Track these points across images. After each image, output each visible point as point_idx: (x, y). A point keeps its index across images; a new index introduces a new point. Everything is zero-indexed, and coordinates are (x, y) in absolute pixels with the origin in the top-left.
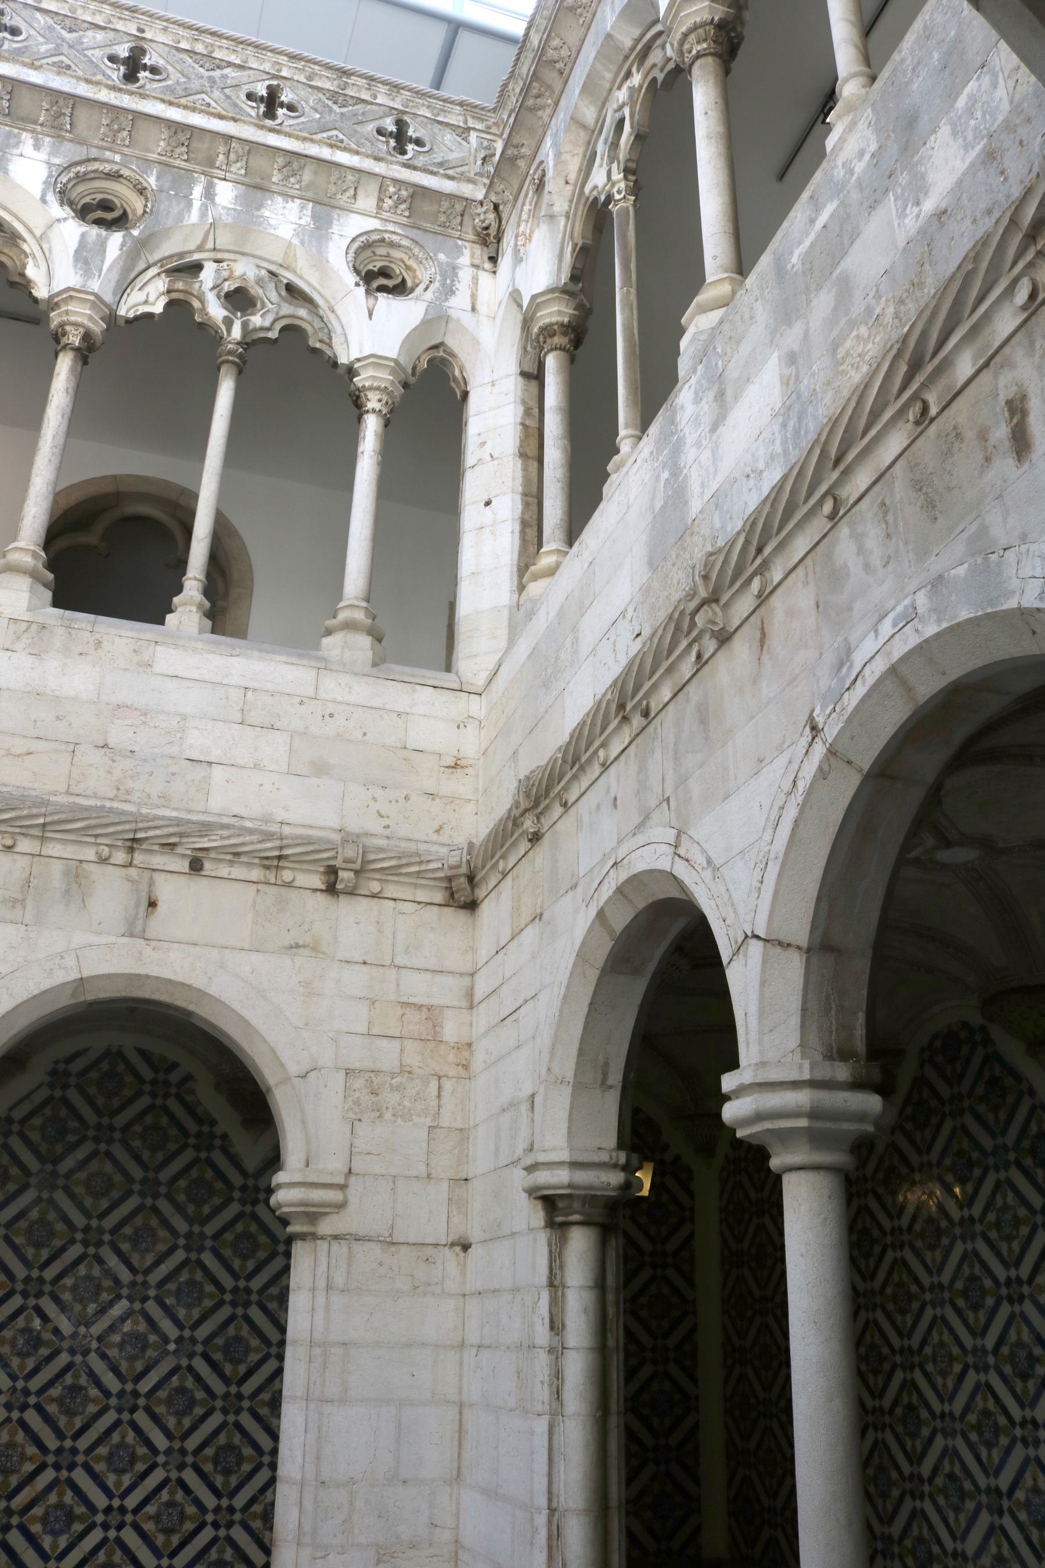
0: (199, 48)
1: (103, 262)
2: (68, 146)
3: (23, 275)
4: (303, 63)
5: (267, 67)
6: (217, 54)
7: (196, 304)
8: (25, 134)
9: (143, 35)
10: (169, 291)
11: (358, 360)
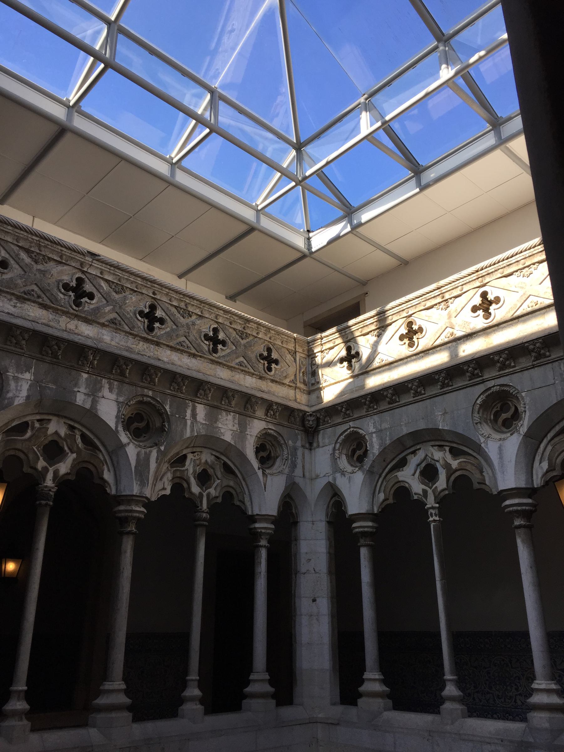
0: (182, 305)
1: (149, 473)
2: (126, 387)
3: (102, 479)
4: (230, 315)
5: (213, 317)
6: (190, 309)
7: (185, 485)
8: (104, 380)
9: (156, 297)
10: (173, 479)
11: (257, 515)
